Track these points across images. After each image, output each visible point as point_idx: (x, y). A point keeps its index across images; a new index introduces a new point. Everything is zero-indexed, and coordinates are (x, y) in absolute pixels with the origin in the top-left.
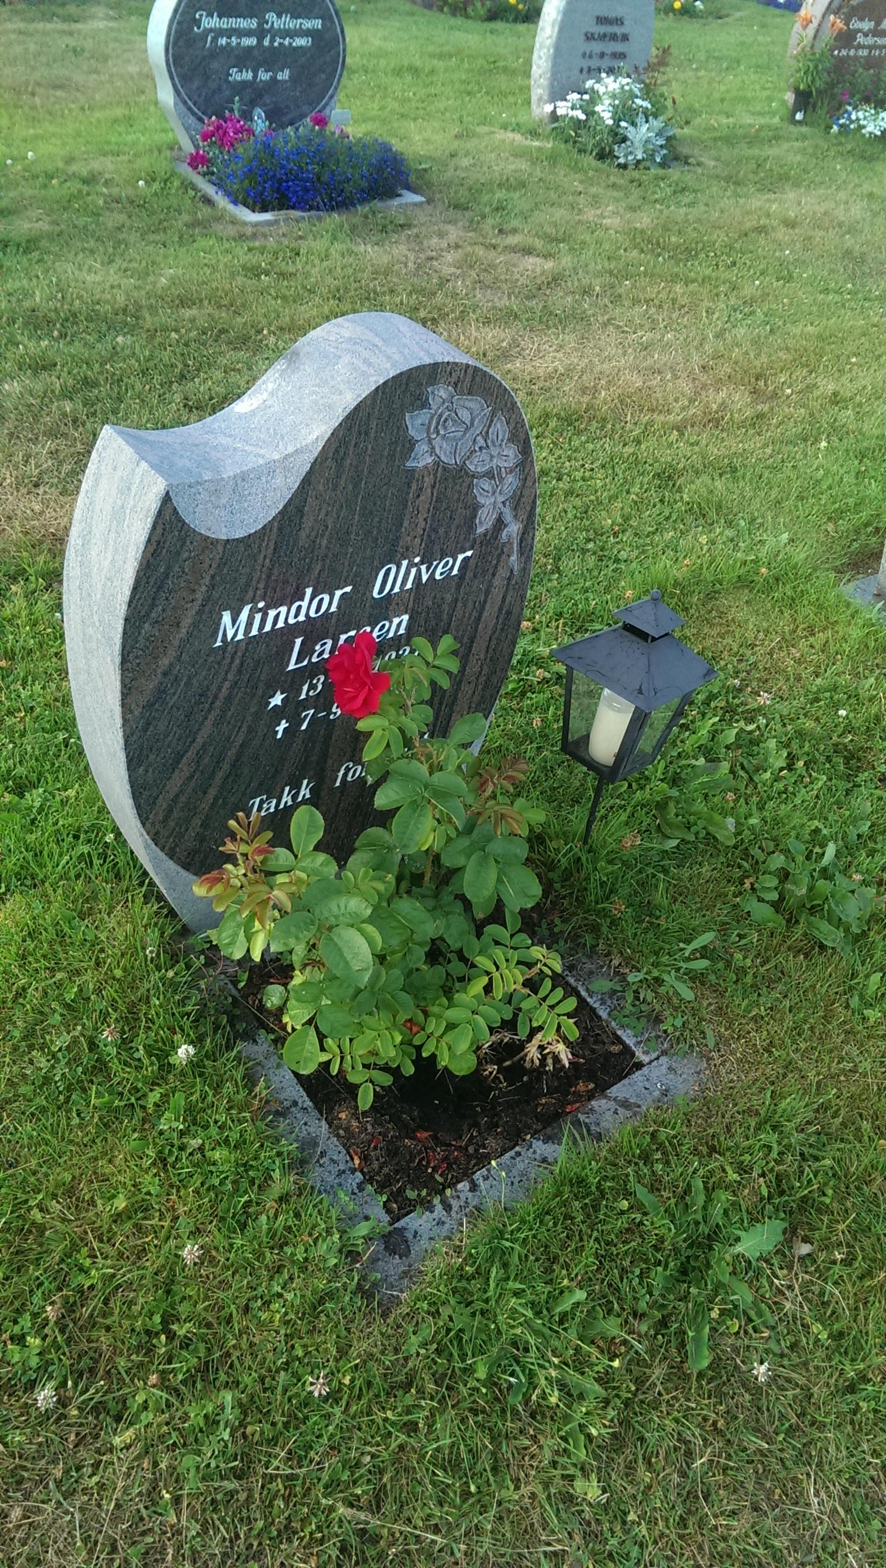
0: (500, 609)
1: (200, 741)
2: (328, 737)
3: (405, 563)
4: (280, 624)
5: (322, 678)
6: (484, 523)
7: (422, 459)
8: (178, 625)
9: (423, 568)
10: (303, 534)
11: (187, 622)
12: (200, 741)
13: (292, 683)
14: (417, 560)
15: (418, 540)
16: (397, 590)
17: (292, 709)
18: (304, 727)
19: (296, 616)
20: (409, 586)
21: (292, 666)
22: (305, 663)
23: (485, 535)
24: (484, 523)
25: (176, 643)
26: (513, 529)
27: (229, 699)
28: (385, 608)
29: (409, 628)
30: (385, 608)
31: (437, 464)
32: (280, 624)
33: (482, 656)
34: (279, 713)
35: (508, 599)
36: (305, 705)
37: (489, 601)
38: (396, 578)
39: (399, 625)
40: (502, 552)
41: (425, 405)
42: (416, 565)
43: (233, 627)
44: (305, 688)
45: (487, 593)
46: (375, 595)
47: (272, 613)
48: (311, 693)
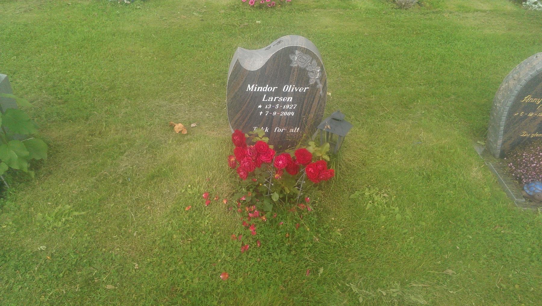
0: (318, 103)
1: (243, 109)
2: (272, 120)
4: (261, 90)
6: (312, 82)
7: (294, 65)
10: (266, 74)
11: (241, 84)
12: (243, 109)
13: (264, 104)
17: (263, 109)
19: (265, 89)
23: (312, 85)
24: (312, 82)
26: (320, 86)
27: (249, 102)
28: (286, 94)
30: (286, 94)
31: (298, 66)
32: (261, 90)
34: (260, 110)
38: (288, 88)
40: (317, 90)
41: (294, 54)
43: (250, 88)
45: (314, 99)
47: (259, 88)
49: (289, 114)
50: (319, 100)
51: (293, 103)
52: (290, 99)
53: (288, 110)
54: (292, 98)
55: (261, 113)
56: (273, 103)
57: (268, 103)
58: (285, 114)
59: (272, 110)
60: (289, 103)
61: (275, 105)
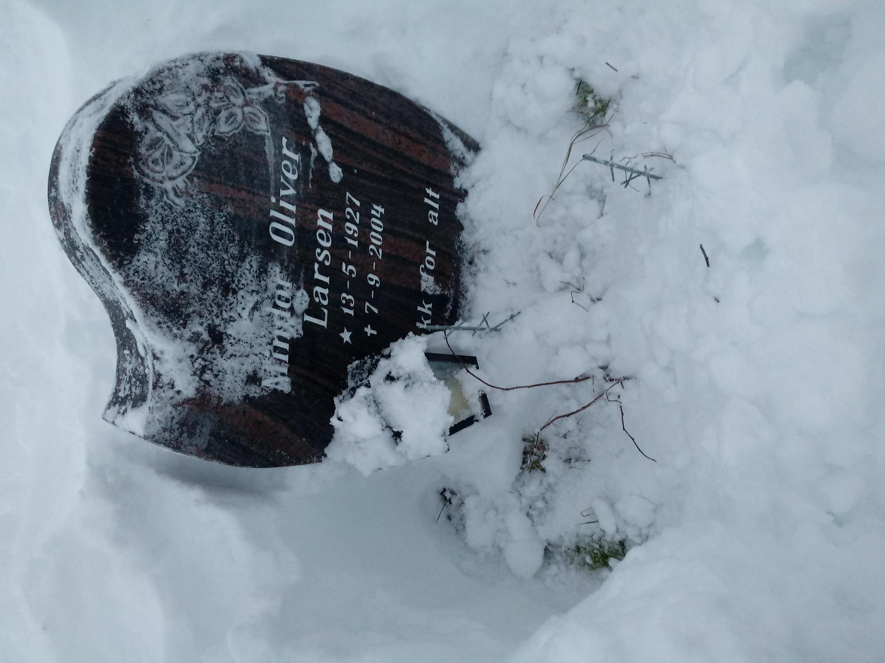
0: (346, 105)
3: (273, 213)
5: (344, 295)
8: (259, 423)
9: (283, 193)
14: (273, 200)
15: (256, 199)
16: (292, 221)
18: (376, 311)
20: (293, 208)
21: (324, 323)
22: (326, 311)
25: (273, 423)
29: (328, 209)
30: (306, 235)
33: (380, 128)
35: (341, 96)
36: (358, 309)
37: (334, 118)
39: (325, 219)
42: (278, 201)
44: (346, 310)
46: (289, 244)
48: (352, 305)
49: (377, 225)
50: (338, 101)
51: (338, 208)
52: (324, 218)
53: (365, 227)
54: (321, 212)
55: (369, 331)
56: (337, 285)
57: (335, 304)
58: (376, 240)
59: (360, 287)
60: (339, 222)
61: (346, 278)
